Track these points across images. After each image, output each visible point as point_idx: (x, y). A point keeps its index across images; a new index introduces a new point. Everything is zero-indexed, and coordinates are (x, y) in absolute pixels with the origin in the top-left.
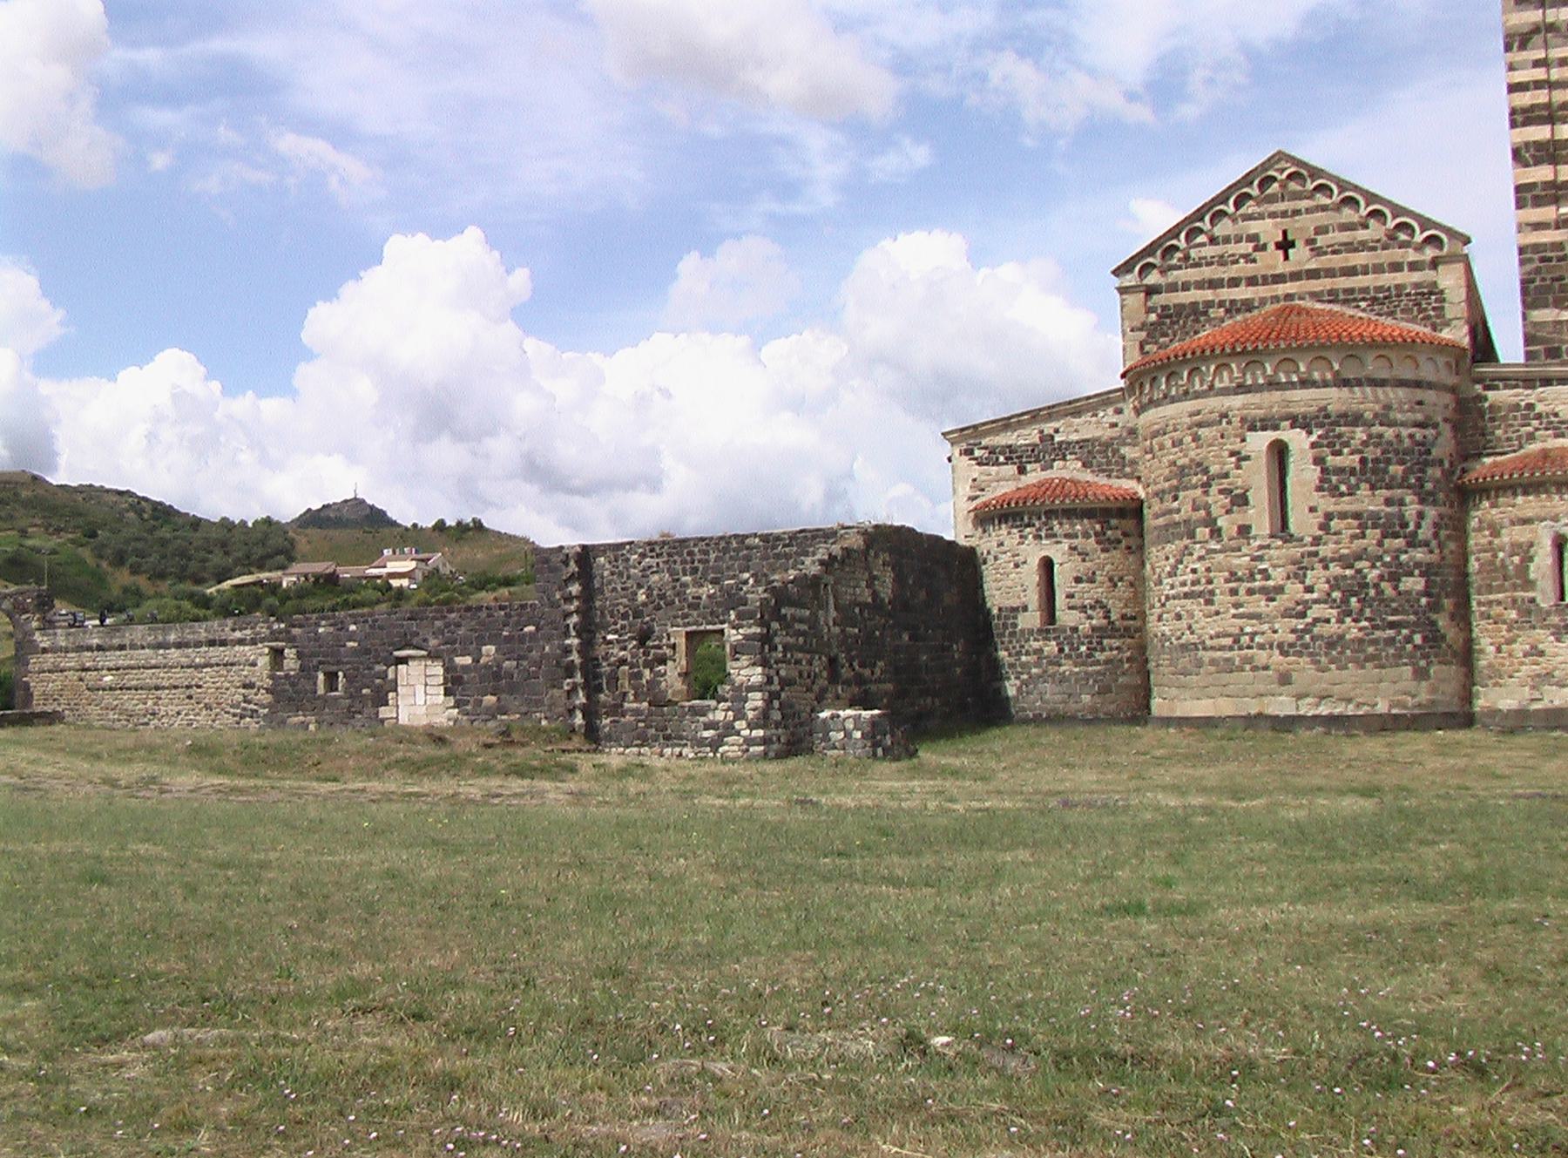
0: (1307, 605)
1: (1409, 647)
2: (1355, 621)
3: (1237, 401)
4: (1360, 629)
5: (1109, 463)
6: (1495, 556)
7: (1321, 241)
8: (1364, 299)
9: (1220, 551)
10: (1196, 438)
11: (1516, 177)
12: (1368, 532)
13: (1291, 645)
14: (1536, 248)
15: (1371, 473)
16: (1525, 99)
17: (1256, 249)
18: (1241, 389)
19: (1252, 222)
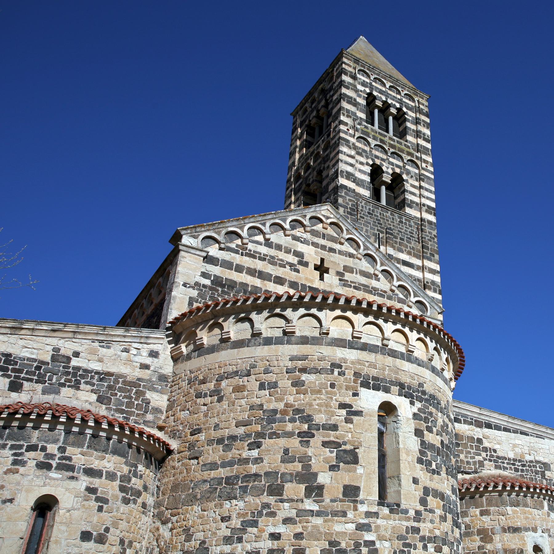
3: (351, 355)
5: (130, 405)
9: (319, 514)
10: (297, 383)
18: (354, 344)
19: (299, 243)
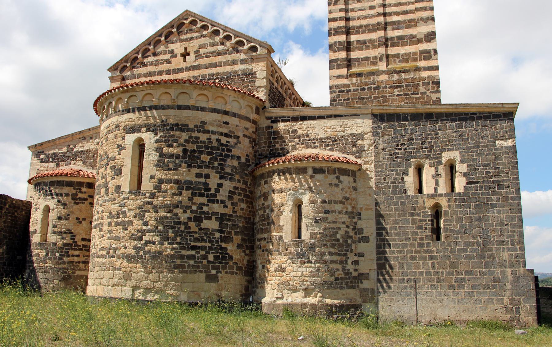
0: (143, 232)
1: (205, 262)
2: (169, 244)
4: (173, 249)
6: (265, 212)
7: (202, 51)
8: (217, 79)
11: (330, 56)
12: (184, 192)
13: (133, 257)
14: (337, 86)
15: (189, 158)
16: (335, 25)
17: (172, 57)
